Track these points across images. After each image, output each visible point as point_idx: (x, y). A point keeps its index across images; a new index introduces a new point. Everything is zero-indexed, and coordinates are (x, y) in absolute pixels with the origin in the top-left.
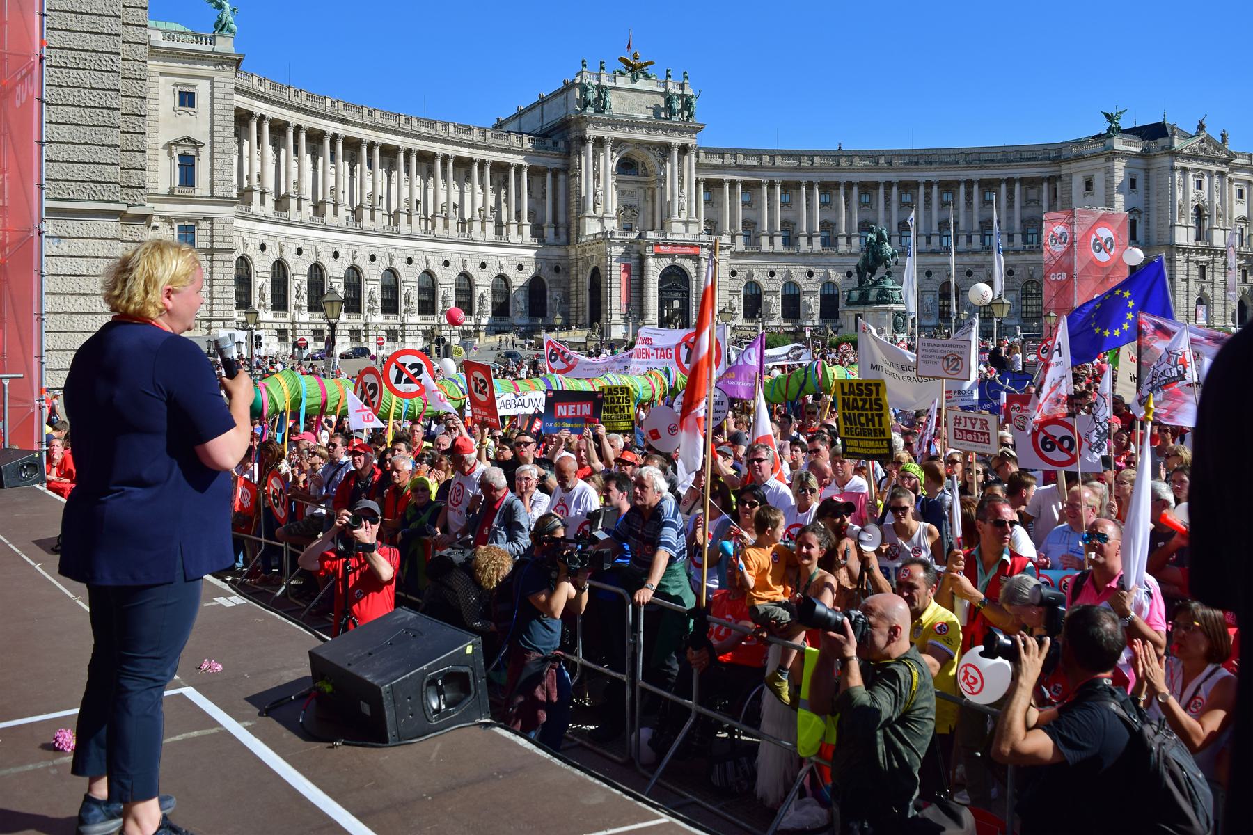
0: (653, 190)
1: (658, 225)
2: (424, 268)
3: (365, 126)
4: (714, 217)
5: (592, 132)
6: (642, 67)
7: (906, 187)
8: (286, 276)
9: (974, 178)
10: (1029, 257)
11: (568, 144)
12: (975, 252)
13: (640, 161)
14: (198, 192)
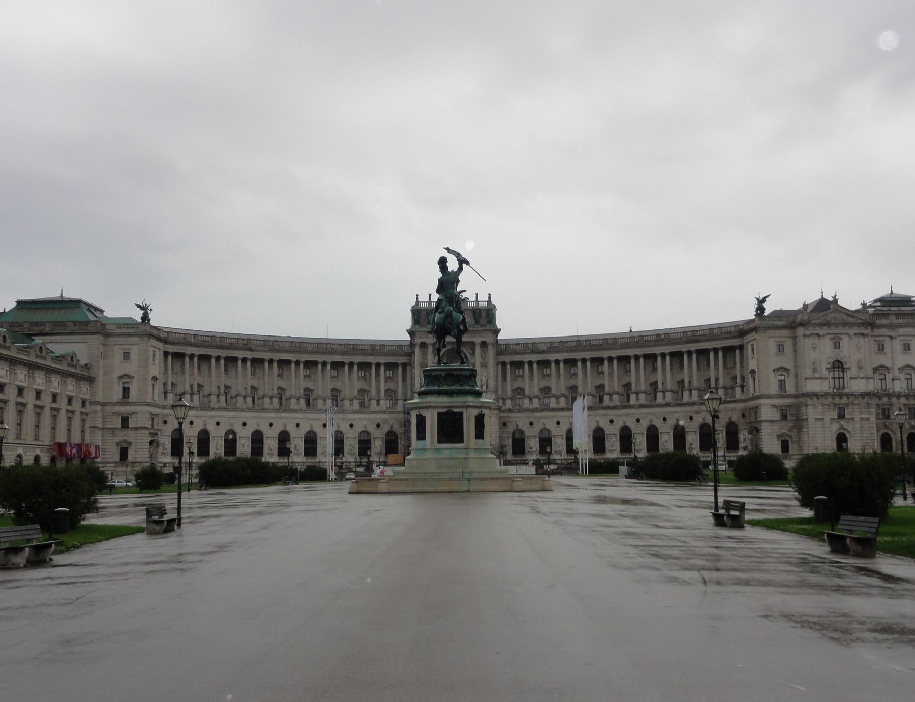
3: (266, 351)
12: (693, 404)
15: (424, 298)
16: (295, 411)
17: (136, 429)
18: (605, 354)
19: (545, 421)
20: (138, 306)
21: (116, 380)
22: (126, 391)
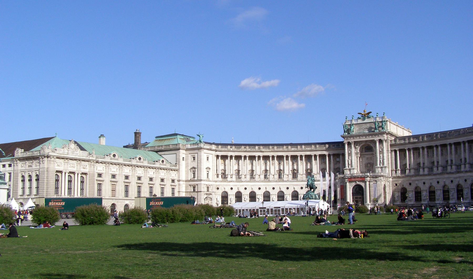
7: (444, 146)
14: (195, 179)
16: (286, 181)
17: (198, 192)
19: (417, 182)
20: (198, 135)
21: (189, 171)
22: (194, 174)
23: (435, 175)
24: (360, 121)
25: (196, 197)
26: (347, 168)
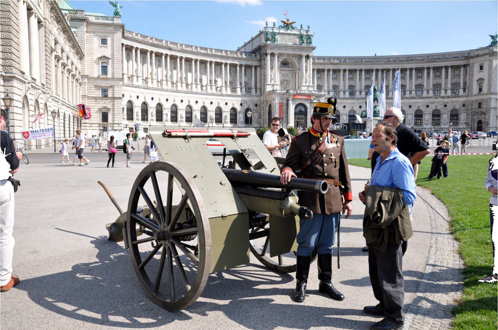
0: (296, 73)
1: (297, 87)
2: (188, 104)
3: (178, 51)
4: (321, 84)
5: (269, 51)
6: (290, 24)
8: (147, 108)
9: (430, 66)
10: (454, 99)
11: (261, 56)
12: (430, 98)
13: (290, 62)
14: (108, 77)
15: (270, 25)
18: (375, 67)
23: (358, 99)
24: (282, 31)
25: (109, 106)
26: (269, 82)
